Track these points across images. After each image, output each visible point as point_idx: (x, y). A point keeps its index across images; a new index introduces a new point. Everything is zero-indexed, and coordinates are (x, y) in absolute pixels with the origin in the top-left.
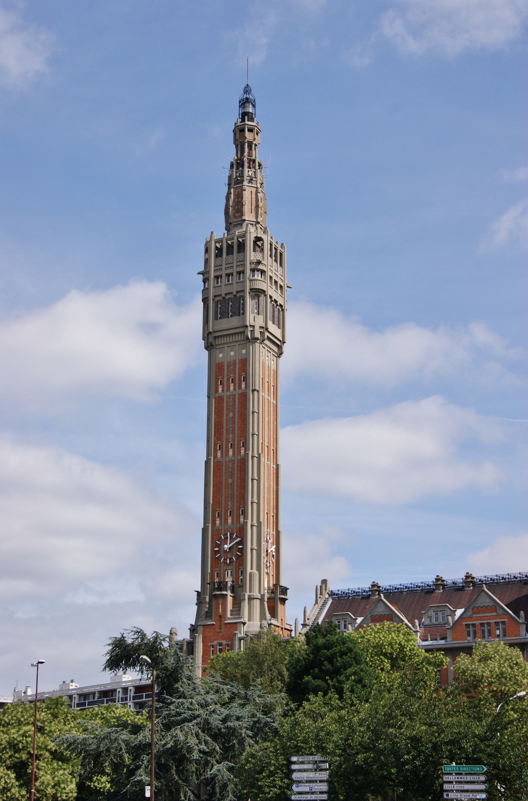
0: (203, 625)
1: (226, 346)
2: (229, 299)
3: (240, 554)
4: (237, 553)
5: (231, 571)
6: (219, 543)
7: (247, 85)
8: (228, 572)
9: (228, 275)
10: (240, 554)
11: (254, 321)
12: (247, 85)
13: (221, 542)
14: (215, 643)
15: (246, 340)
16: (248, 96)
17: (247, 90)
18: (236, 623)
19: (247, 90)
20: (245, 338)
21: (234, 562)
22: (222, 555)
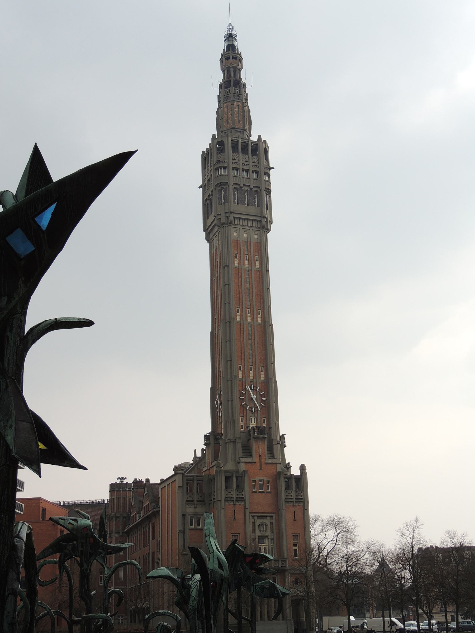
0: (245, 462)
1: (241, 227)
2: (245, 190)
3: (264, 405)
4: (261, 404)
5: (254, 419)
6: (245, 393)
7: (230, 24)
8: (251, 419)
9: (243, 170)
10: (264, 405)
11: (267, 215)
12: (230, 24)
13: (245, 393)
14: (257, 479)
15: (259, 228)
16: (230, 33)
17: (230, 27)
18: (276, 463)
19: (230, 27)
20: (259, 226)
21: (258, 411)
22: (247, 404)
